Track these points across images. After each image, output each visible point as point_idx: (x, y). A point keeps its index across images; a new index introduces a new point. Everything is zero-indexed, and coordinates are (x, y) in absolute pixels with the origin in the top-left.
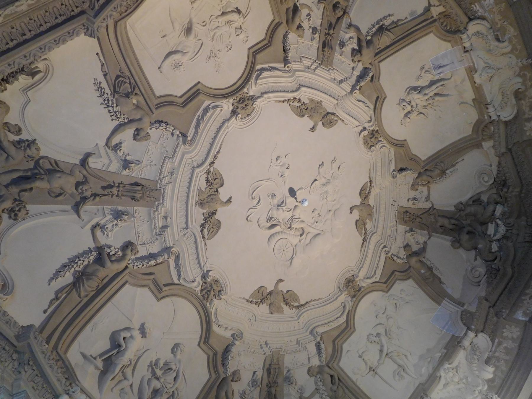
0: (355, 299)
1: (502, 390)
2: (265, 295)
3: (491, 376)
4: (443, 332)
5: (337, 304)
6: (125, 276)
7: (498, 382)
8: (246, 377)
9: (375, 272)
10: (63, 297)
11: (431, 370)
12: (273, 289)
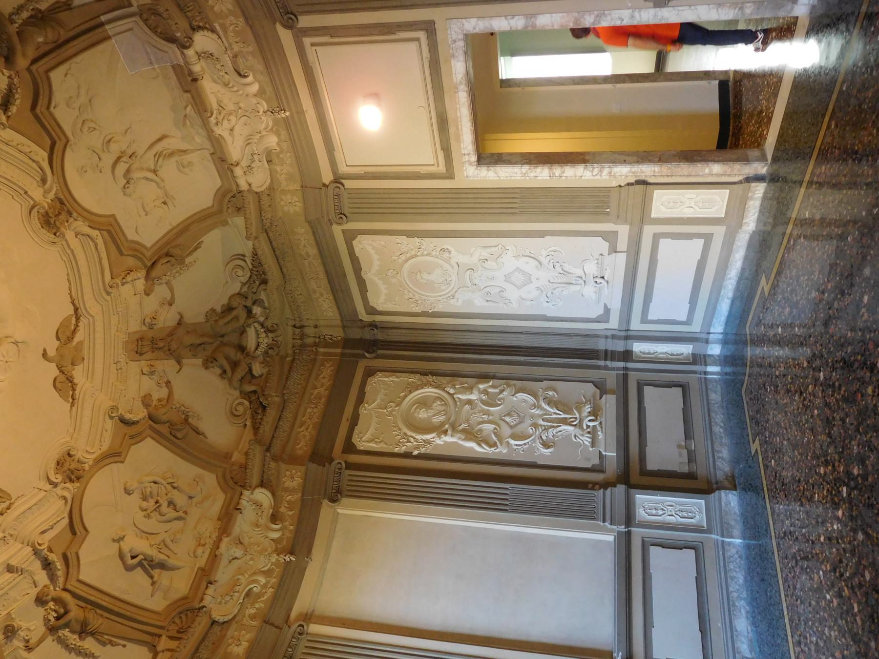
0: (75, 214)
1: (275, 80)
2: (62, 378)
3: (255, 88)
4: (158, 71)
5: (74, 243)
6: (72, 585)
7: (269, 89)
8: (148, 384)
9: (34, 161)
10: (106, 637)
11: (203, 133)
12: (54, 365)
